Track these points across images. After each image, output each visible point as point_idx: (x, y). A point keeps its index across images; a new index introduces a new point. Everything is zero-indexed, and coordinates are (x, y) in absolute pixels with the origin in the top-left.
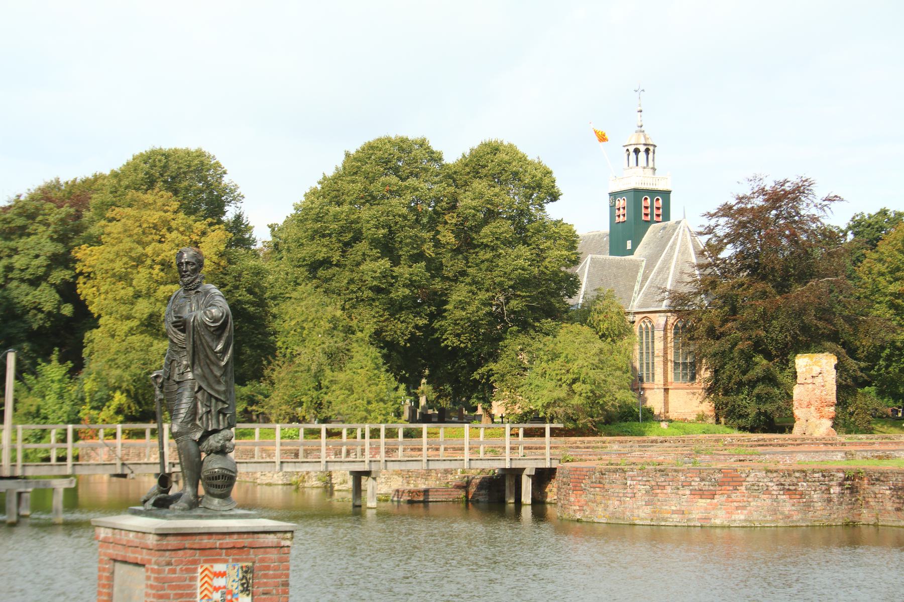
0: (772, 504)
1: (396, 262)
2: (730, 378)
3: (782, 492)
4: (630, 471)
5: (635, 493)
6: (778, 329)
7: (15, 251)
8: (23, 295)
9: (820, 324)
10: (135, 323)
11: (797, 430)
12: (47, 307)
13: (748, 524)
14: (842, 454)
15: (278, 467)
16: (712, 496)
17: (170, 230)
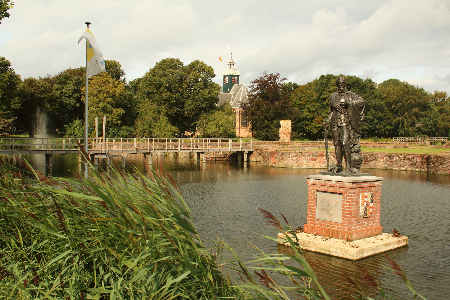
1: (172, 93)
2: (258, 126)
7: (63, 88)
8: (67, 101)
9: (282, 112)
10: (99, 109)
11: (280, 140)
12: (73, 104)
14: (318, 147)
15: (179, 151)
16: (316, 160)
17: (109, 83)
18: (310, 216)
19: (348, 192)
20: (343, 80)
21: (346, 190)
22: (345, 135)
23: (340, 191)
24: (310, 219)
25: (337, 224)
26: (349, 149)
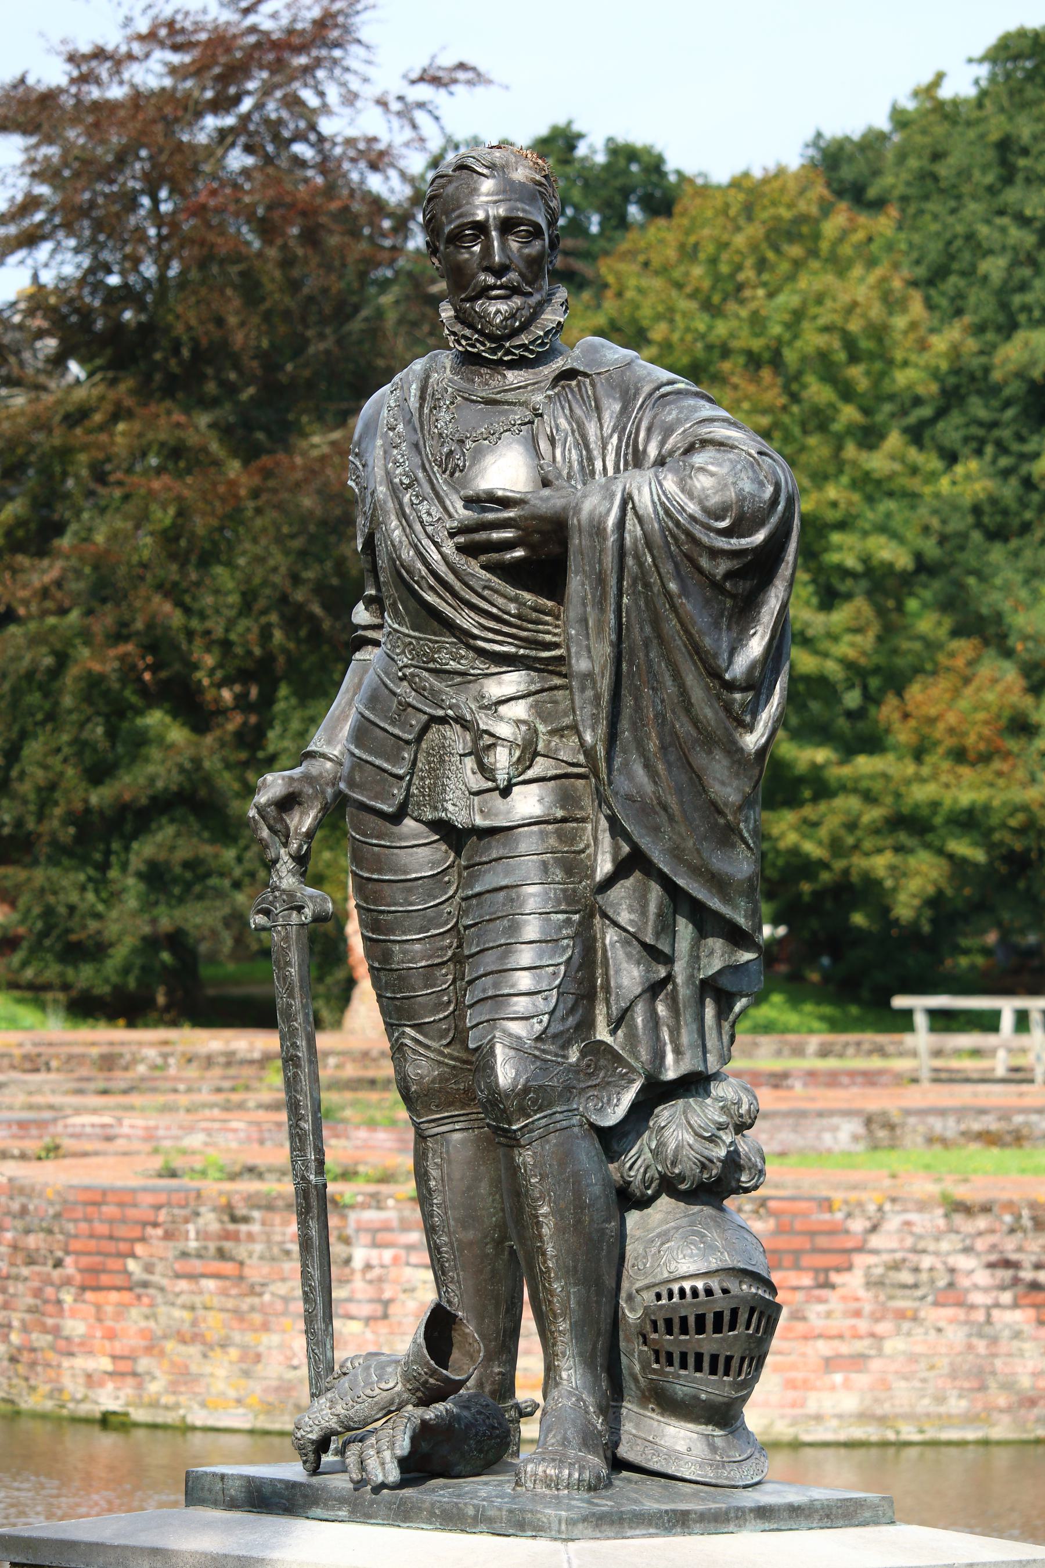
0: (970, 1347)
3: (1006, 1297)
4: (364, 1206)
5: (386, 1303)
6: (233, 599)
13: (871, 1433)
14: (849, 1128)
20: (509, 190)
22: (526, 956)
26: (587, 1152)
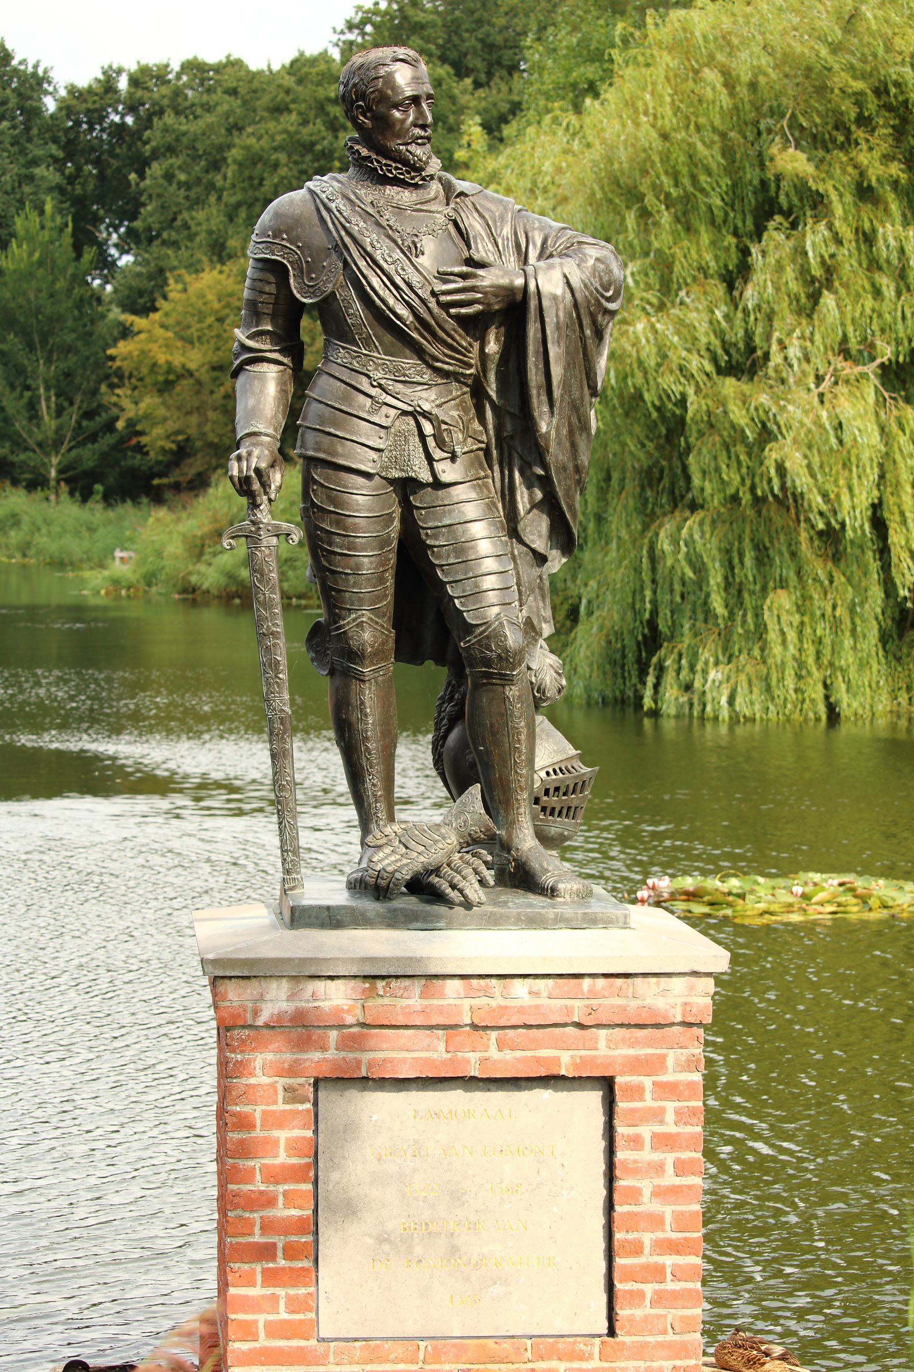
18: (261, 1319)
19: (670, 1061)
21: (649, 1043)
23: (584, 1061)
24: (263, 1341)
25: (561, 1344)
